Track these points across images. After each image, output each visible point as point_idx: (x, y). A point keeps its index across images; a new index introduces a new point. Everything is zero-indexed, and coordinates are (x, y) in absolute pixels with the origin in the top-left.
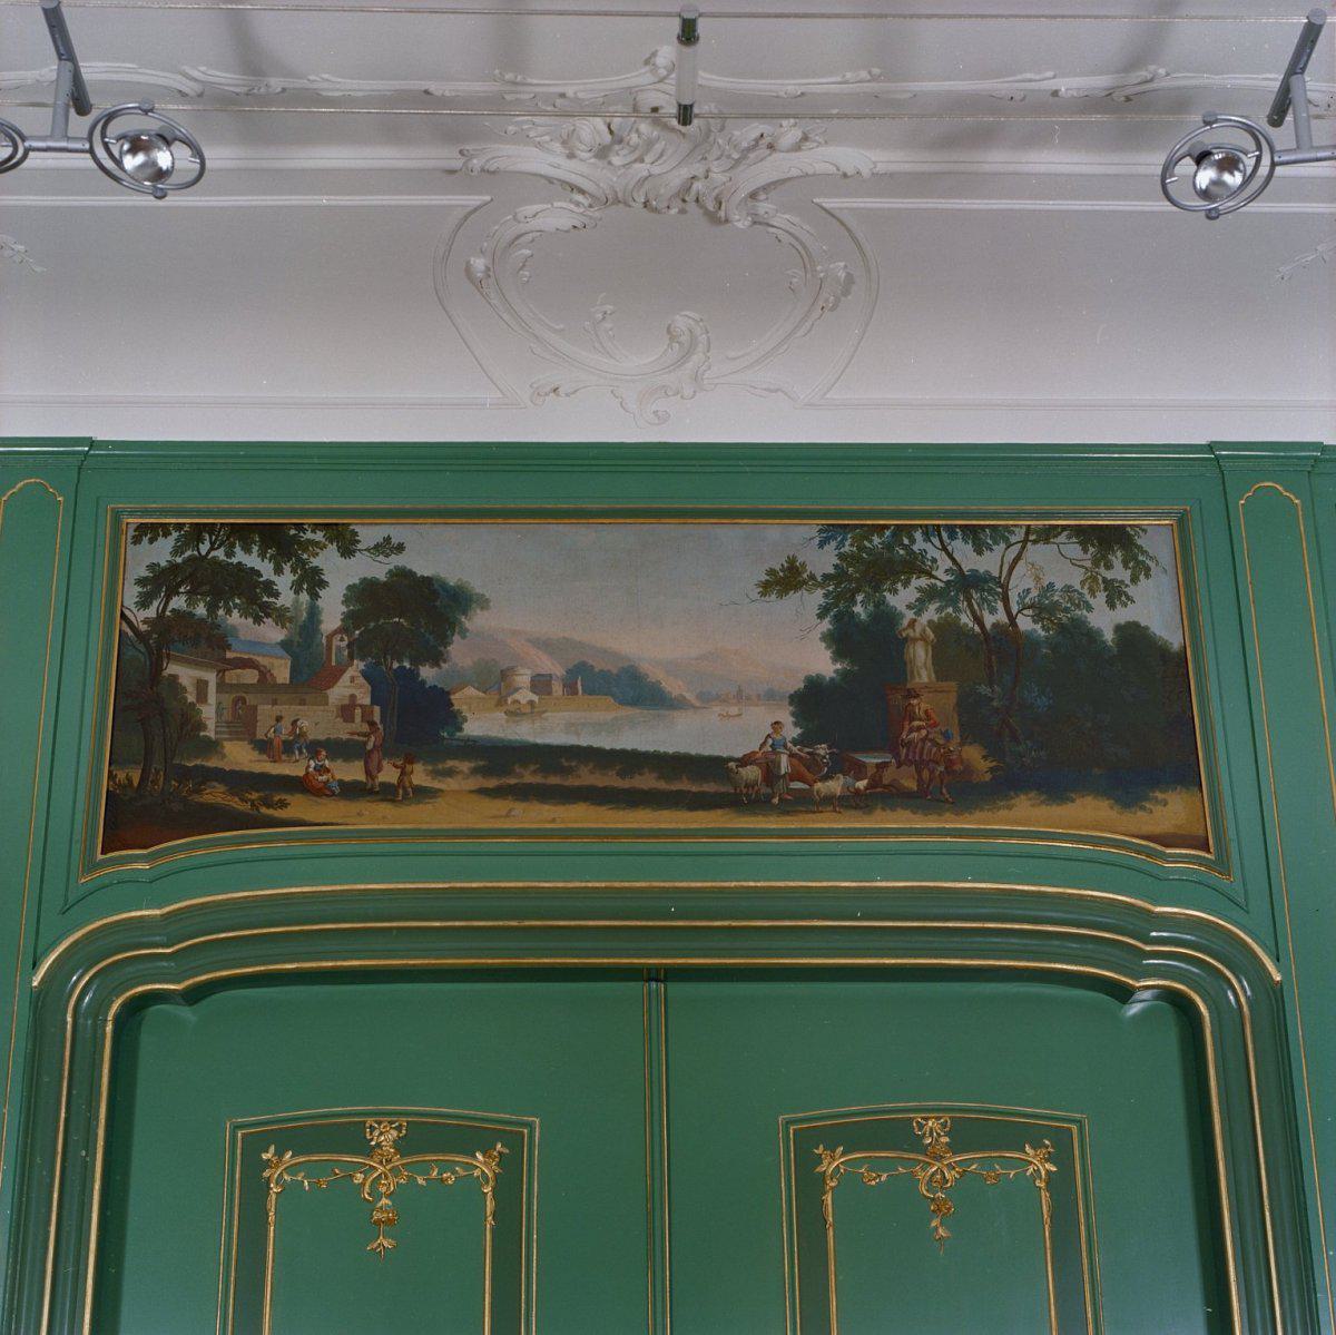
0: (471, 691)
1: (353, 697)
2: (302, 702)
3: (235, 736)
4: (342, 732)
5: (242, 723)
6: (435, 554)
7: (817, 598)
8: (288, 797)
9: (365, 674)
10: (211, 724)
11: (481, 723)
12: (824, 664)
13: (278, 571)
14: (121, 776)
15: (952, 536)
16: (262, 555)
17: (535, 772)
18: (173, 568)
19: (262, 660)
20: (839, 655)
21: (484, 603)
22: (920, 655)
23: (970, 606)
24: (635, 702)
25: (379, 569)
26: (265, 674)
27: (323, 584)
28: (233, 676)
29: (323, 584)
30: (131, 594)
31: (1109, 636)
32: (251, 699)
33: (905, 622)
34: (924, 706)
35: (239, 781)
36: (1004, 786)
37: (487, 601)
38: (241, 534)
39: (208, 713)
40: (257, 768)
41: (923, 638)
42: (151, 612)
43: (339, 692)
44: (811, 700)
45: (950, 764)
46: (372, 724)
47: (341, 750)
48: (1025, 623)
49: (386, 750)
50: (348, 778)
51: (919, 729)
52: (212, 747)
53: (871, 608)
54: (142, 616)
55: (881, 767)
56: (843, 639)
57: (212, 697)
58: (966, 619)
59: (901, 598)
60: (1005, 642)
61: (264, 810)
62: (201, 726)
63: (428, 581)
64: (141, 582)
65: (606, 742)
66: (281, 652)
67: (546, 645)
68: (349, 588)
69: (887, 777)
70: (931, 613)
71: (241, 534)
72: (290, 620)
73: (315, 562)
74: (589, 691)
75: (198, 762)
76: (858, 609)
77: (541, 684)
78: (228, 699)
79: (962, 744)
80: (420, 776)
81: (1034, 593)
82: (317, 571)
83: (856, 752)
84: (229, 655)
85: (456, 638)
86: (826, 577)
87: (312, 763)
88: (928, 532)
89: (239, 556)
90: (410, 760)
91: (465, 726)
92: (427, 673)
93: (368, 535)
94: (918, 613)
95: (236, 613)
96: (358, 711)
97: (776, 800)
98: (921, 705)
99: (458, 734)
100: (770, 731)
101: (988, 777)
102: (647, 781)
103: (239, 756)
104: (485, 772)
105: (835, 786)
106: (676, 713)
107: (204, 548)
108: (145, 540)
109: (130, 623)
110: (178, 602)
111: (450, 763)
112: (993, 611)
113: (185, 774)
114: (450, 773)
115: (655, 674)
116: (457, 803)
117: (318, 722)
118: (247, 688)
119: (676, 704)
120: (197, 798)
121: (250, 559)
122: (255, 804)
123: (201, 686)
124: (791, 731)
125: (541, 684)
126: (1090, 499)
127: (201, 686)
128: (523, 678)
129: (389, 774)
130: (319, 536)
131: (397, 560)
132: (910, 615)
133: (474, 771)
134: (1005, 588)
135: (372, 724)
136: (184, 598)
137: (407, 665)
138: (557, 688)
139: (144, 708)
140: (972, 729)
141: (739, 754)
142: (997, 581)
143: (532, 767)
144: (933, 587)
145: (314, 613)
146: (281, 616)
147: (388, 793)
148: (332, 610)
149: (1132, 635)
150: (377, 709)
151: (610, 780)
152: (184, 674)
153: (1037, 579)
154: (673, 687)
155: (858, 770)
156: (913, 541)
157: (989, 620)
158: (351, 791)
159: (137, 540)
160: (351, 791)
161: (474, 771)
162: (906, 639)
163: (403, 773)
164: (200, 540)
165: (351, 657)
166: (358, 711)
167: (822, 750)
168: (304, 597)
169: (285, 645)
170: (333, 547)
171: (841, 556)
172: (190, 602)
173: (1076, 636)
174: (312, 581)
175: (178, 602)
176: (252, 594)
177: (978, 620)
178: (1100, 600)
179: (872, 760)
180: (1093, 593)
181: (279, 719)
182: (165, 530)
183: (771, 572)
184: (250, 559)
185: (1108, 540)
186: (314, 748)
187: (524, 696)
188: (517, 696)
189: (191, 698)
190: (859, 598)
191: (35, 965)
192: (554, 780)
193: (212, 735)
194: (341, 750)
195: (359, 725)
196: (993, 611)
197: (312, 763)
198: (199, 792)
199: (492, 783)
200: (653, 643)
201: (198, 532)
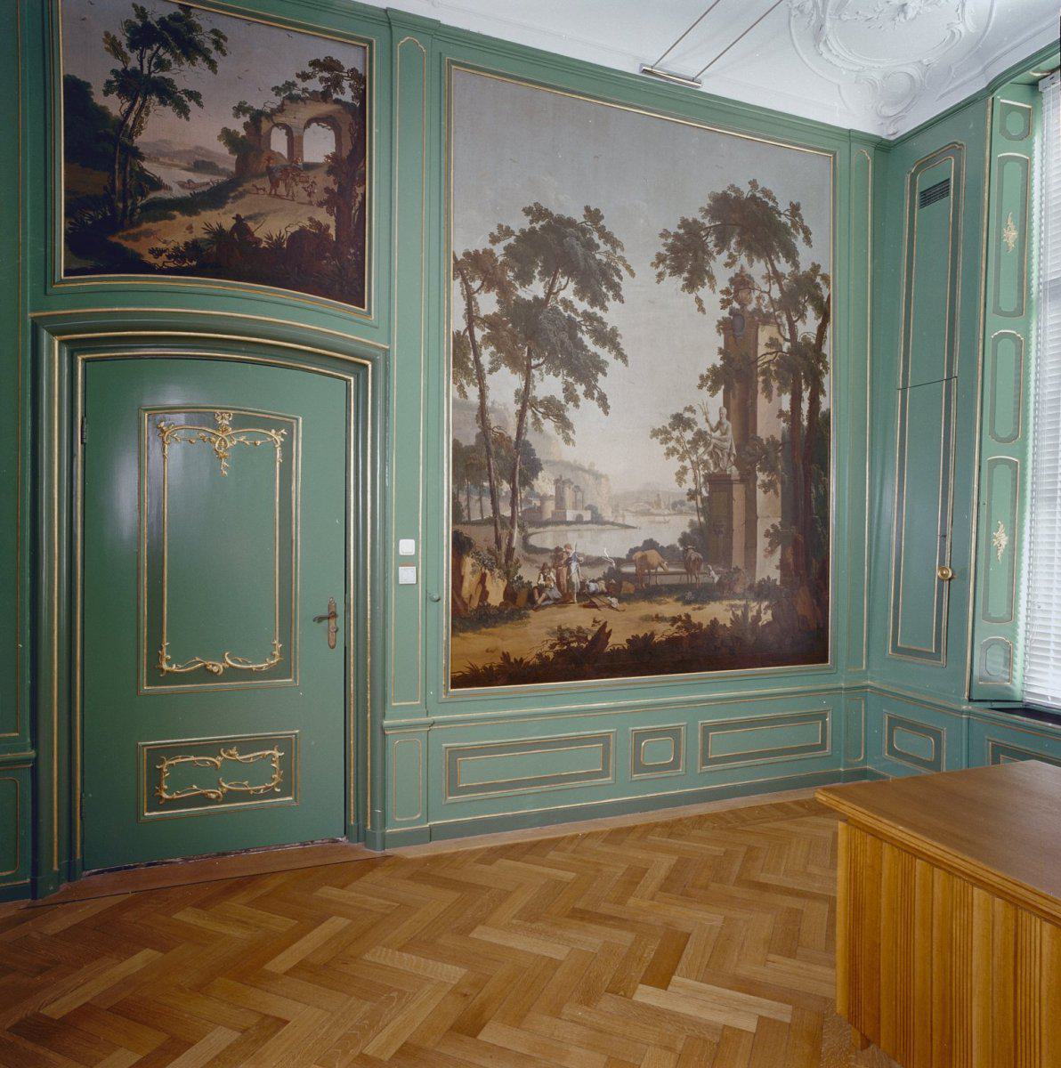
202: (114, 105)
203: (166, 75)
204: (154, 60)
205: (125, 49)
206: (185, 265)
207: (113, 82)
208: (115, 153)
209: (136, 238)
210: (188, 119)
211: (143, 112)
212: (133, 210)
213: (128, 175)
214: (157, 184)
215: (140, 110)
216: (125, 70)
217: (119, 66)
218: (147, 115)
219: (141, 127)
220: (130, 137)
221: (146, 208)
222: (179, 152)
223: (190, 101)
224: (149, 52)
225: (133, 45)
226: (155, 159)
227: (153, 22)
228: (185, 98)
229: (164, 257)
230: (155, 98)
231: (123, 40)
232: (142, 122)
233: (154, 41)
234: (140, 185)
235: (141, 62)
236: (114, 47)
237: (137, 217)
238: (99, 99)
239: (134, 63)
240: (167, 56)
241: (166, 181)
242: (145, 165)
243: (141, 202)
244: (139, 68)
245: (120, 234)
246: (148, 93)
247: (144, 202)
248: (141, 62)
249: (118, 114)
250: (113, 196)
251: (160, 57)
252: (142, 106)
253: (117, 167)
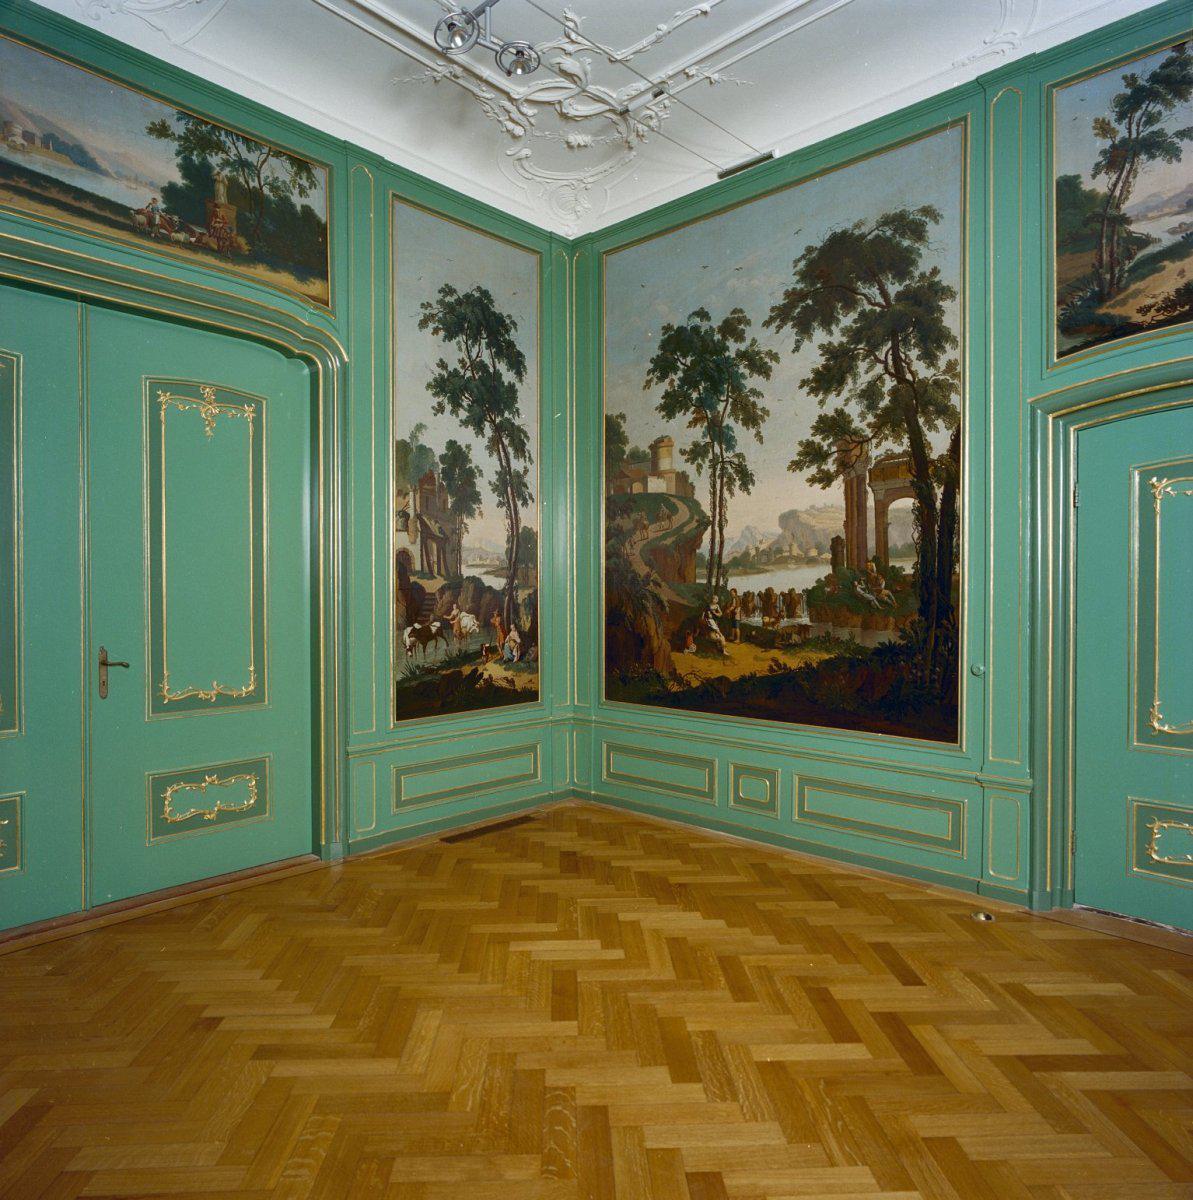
7: (175, 145)
12: (179, 180)
15: (238, 140)
17: (25, 182)
20: (185, 176)
22: (221, 189)
23: (244, 174)
24: (82, 164)
31: (299, 208)
33: (216, 172)
34: (221, 213)
36: (253, 259)
41: (223, 182)
44: (170, 192)
45: (231, 243)
48: (266, 190)
51: (219, 222)
53: (200, 160)
55: (202, 234)
56: (187, 168)
58: (241, 180)
59: (215, 160)
60: (255, 195)
65: (67, 180)
67: (31, 116)
69: (205, 239)
70: (227, 172)
76: (194, 158)
77: (28, 136)
79: (237, 235)
81: (271, 179)
83: (192, 224)
86: (180, 137)
88: (228, 133)
94: (222, 169)
97: (153, 235)
98: (221, 212)
100: (150, 201)
101: (247, 253)
105: (181, 236)
106: (104, 178)
112: (253, 181)
115: (93, 154)
119: (105, 173)
124: (161, 205)
125: (28, 136)
126: (308, 150)
128: (18, 130)
132: (218, 169)
134: (259, 172)
138: (38, 142)
140: (243, 230)
141: (136, 208)
142: (256, 167)
144: (228, 160)
149: (307, 210)
153: (272, 173)
154: (104, 165)
155: (192, 234)
156: (220, 135)
157: (252, 184)
162: (215, 180)
167: (176, 218)
171: (187, 129)
173: (285, 202)
177: (247, 182)
178: (296, 191)
179: (198, 230)
180: (294, 187)
183: (153, 123)
185: (302, 165)
187: (19, 140)
188: (14, 138)
190: (195, 153)
196: (253, 181)
200: (97, 141)
202: (1101, 184)
203: (1155, 128)
204: (1144, 119)
205: (1114, 124)
206: (1177, 312)
207: (1101, 163)
208: (1102, 229)
209: (1124, 302)
210: (1179, 160)
211: (1131, 176)
212: (1121, 276)
213: (1115, 245)
214: (1145, 241)
215: (1127, 177)
216: (1113, 146)
217: (1107, 143)
218: (1134, 177)
219: (1129, 192)
220: (1118, 207)
221: (1132, 270)
222: (1170, 199)
223: (1182, 140)
224: (1138, 114)
225: (1120, 119)
226: (1143, 217)
227: (1145, 83)
228: (1176, 140)
229: (1153, 312)
230: (1143, 157)
231: (1110, 116)
232: (1130, 186)
233: (1143, 102)
234: (1129, 250)
235: (1129, 129)
236: (1103, 128)
237: (1124, 282)
238: (1087, 185)
239: (1122, 131)
240: (1159, 107)
241: (1154, 235)
242: (1133, 228)
243: (1128, 265)
244: (1127, 136)
245: (1108, 304)
246: (1136, 154)
247: (1131, 264)
248: (1129, 129)
249: (1106, 190)
250: (1100, 270)
251: (1150, 112)
252: (1129, 172)
253: (1104, 241)
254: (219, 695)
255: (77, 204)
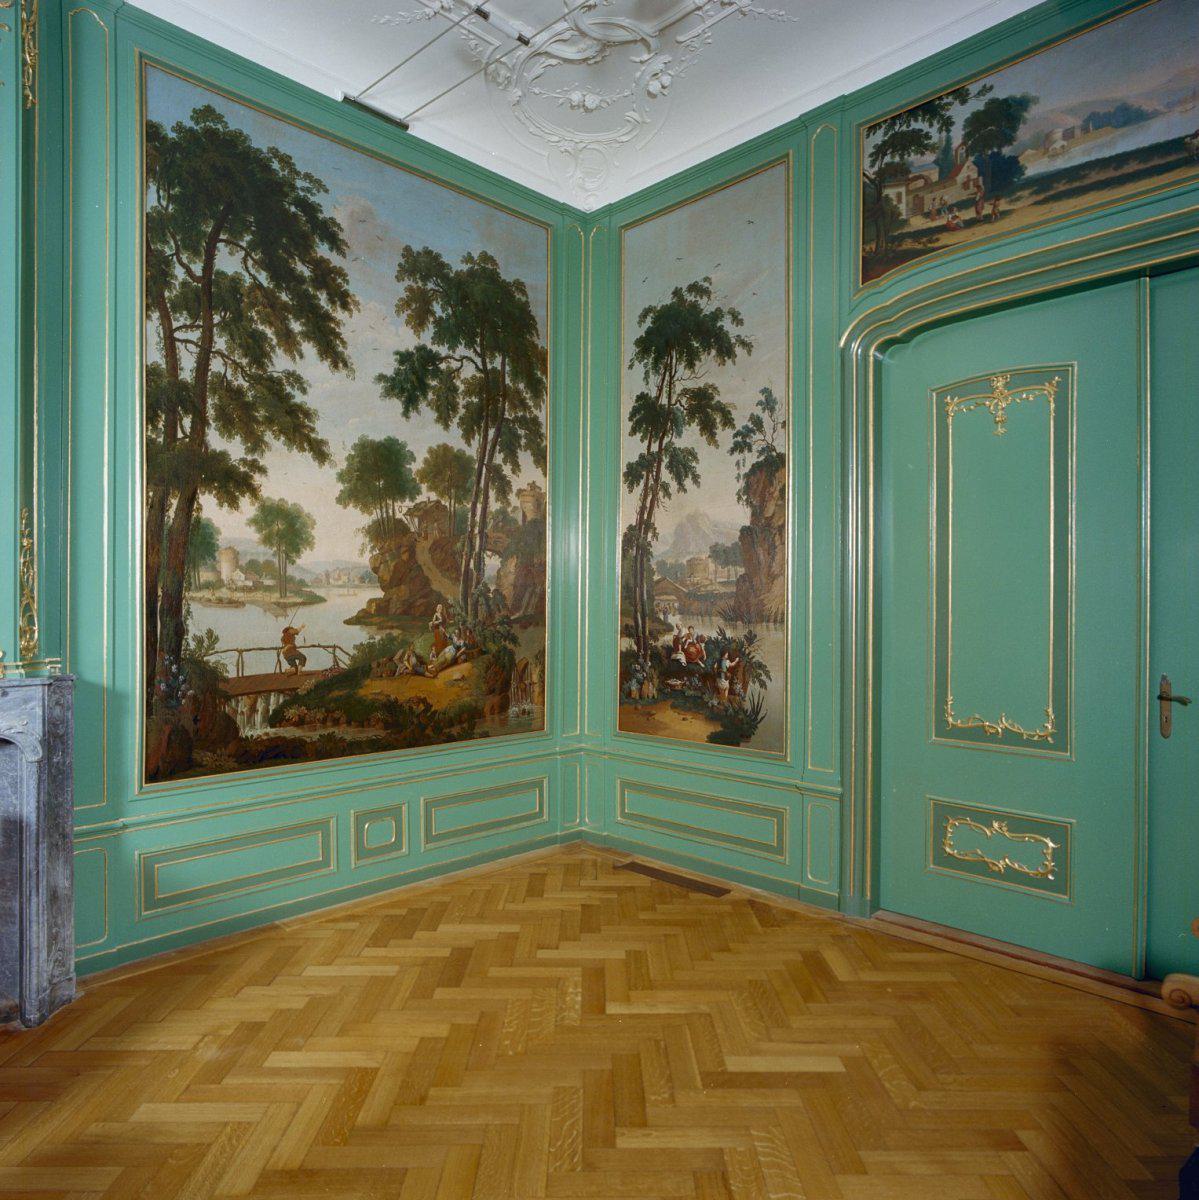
0: (1030, 152)
1: (968, 177)
2: (945, 187)
3: (915, 214)
4: (964, 195)
5: (917, 208)
6: (1005, 87)
8: (940, 236)
9: (974, 163)
10: (904, 212)
11: (1034, 167)
13: (931, 125)
14: (868, 248)
16: (923, 120)
18: (884, 142)
19: (925, 173)
21: (1036, 100)
25: (976, 105)
26: (926, 179)
27: (952, 124)
28: (914, 185)
29: (952, 124)
30: (867, 161)
32: (921, 194)
35: (917, 235)
37: (1038, 99)
38: (913, 113)
39: (903, 207)
40: (925, 227)
42: (876, 168)
43: (961, 178)
46: (978, 187)
47: (962, 205)
49: (985, 198)
50: (967, 217)
52: (906, 222)
54: (871, 172)
57: (904, 200)
61: (929, 245)
62: (900, 214)
63: (1006, 100)
64: (871, 155)
65: (1107, 153)
66: (934, 165)
67: (1071, 111)
68: (966, 120)
71: (913, 113)
72: (937, 148)
73: (948, 114)
74: (1097, 128)
75: (900, 232)
77: (1068, 135)
78: (911, 197)
80: (1003, 205)
82: (949, 118)
84: (911, 176)
85: (1021, 126)
87: (950, 216)
89: (915, 125)
90: (998, 199)
91: (1026, 172)
92: (1006, 151)
93: (974, 88)
95: (912, 154)
96: (971, 183)
99: (1023, 177)
102: (1132, 167)
103: (918, 223)
104: (1036, 193)
106: (1149, 121)
107: (897, 128)
108: (871, 134)
109: (867, 177)
110: (887, 159)
111: (1019, 194)
113: (894, 239)
114: (1018, 199)
116: (1023, 211)
117: (952, 194)
118: (919, 189)
119: (1155, 114)
120: (900, 248)
121: (919, 125)
122: (926, 243)
123: (899, 196)
127: (899, 196)
129: (987, 210)
130: (950, 99)
131: (990, 96)
133: (1031, 194)
135: (978, 187)
136: (889, 156)
137: (995, 150)
138: (1078, 132)
139: (876, 213)
143: (1064, 181)
145: (949, 140)
146: (933, 148)
147: (988, 219)
148: (957, 134)
150: (981, 179)
151: (1111, 173)
152: (890, 192)
154: (1147, 107)
158: (970, 224)
159: (868, 136)
160: (970, 224)
161: (1031, 194)
163: (995, 206)
164: (895, 124)
165: (967, 156)
166: (971, 183)
168: (944, 134)
169: (936, 162)
170: (957, 102)
172: (893, 157)
174: (947, 123)
175: (887, 159)
176: (918, 141)
181: (934, 200)
182: (879, 125)
184: (919, 125)
186: (950, 209)
189: (895, 203)
191: (840, 339)
192: (1077, 184)
193: (904, 217)
194: (962, 205)
195: (972, 189)
197: (950, 216)
198: (900, 245)
199: (1042, 197)
201: (893, 119)
254: (1005, 730)
255: (1118, 173)
